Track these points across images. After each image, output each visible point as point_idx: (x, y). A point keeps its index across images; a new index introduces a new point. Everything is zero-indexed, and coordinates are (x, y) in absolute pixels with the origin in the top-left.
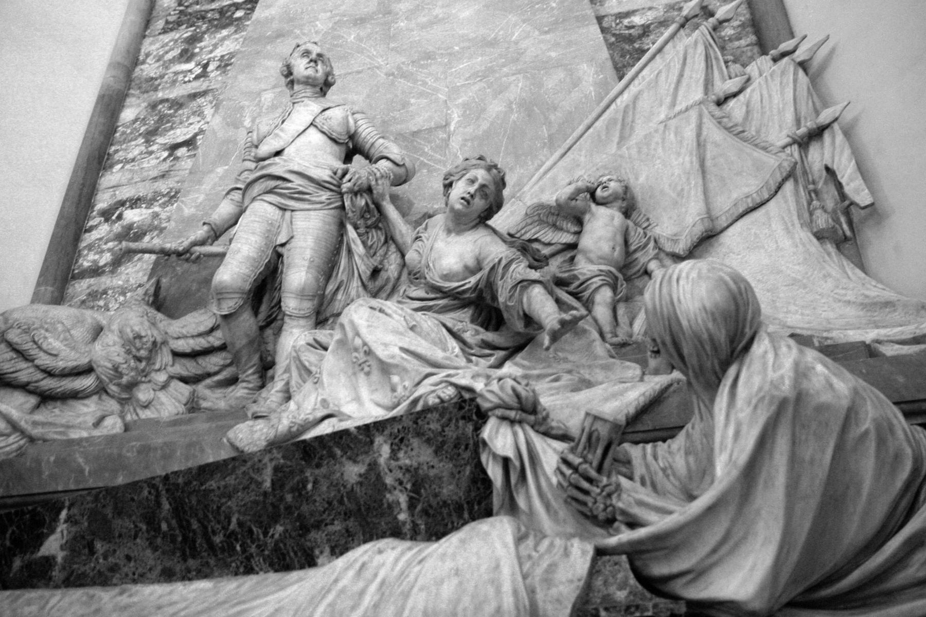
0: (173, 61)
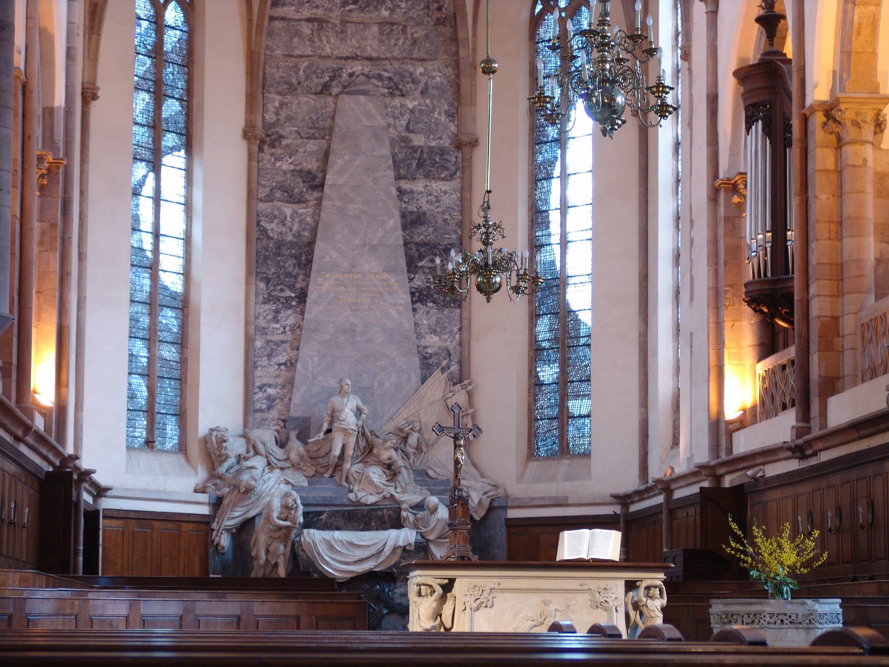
0: (270, 320)
